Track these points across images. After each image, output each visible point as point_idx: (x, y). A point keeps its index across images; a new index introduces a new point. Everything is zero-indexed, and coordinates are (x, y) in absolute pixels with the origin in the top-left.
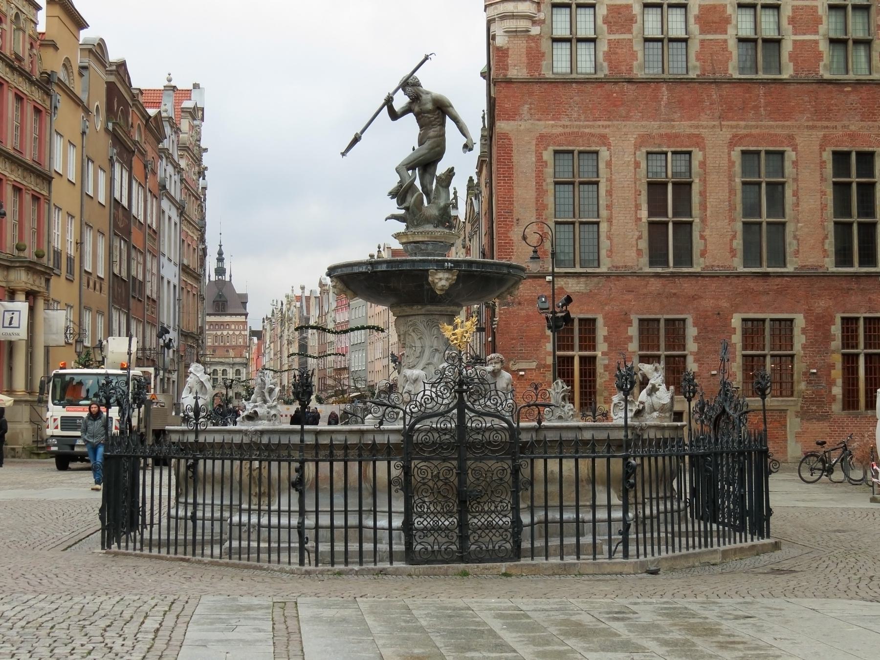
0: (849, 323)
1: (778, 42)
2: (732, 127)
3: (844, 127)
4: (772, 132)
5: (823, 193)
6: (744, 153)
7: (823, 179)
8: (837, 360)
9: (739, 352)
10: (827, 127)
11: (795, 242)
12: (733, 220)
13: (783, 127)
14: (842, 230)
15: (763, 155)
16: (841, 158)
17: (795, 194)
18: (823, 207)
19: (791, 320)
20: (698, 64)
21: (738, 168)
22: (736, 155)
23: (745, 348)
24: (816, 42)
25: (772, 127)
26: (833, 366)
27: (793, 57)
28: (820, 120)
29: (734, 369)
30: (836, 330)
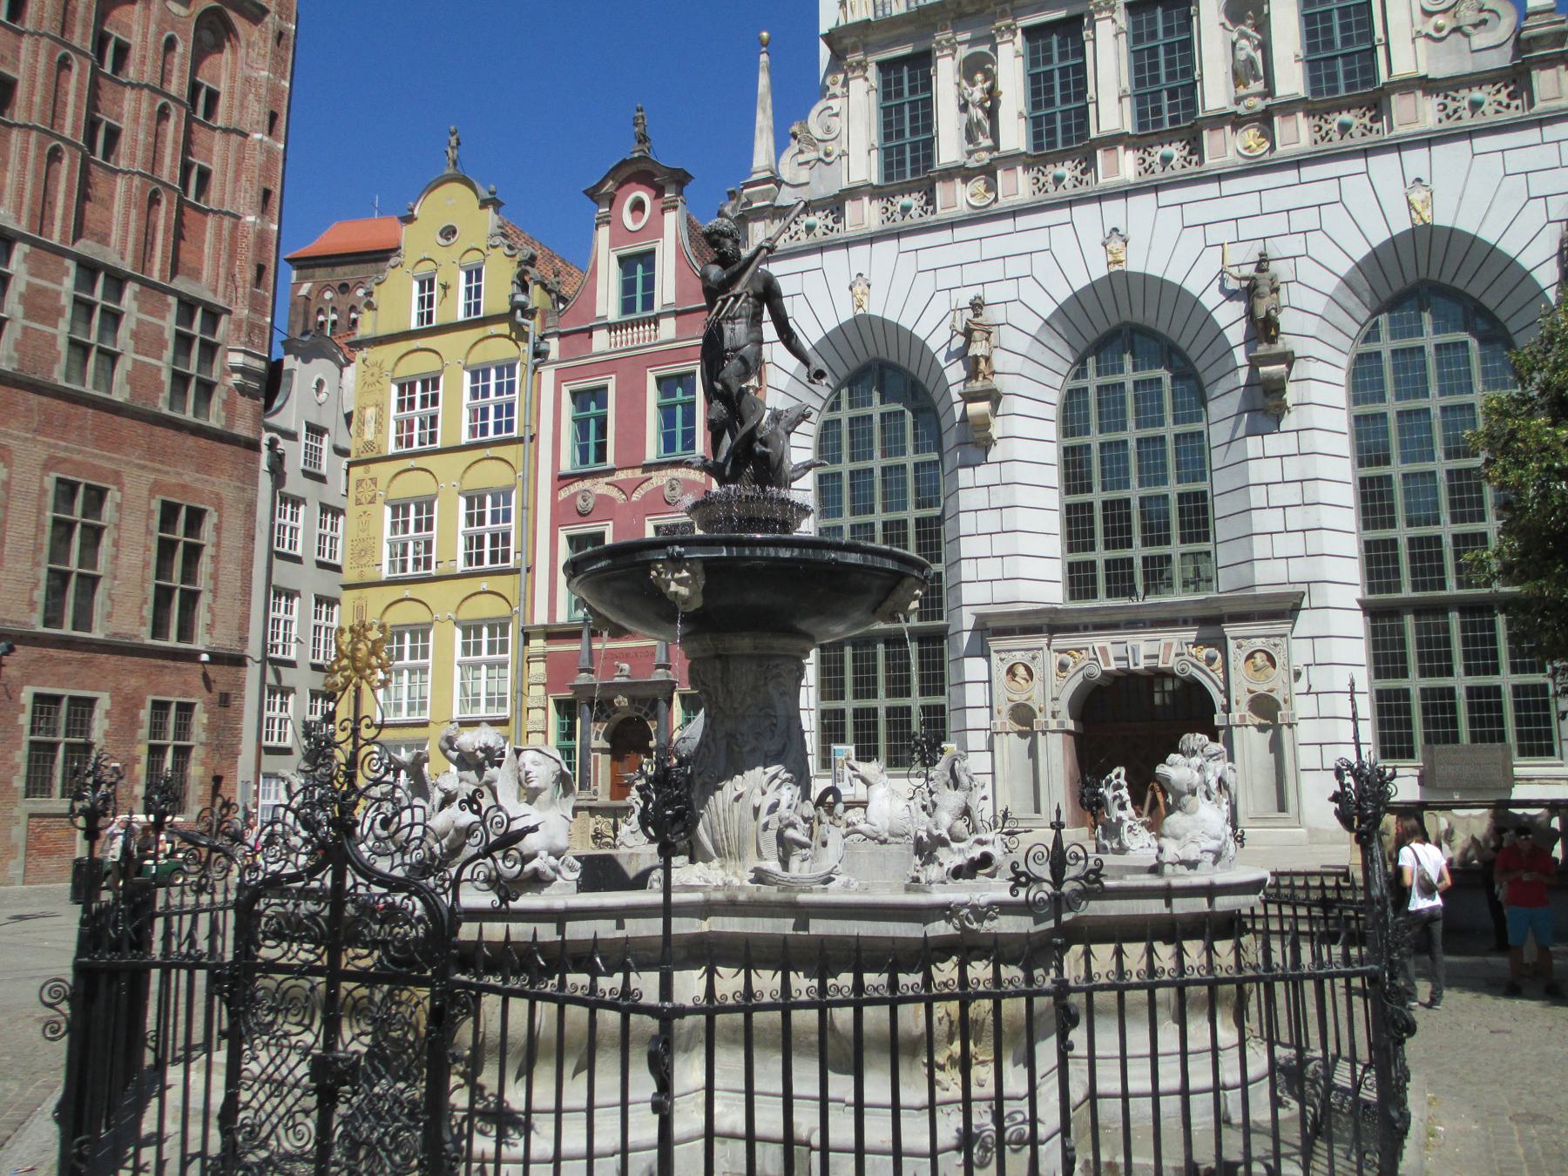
0: (160, 707)
1: (113, 357)
2: (50, 446)
3: (178, 474)
4: (97, 462)
5: (147, 548)
6: (59, 481)
7: (149, 532)
8: (142, 751)
9: (26, 737)
10: (159, 471)
11: (109, 603)
12: (37, 564)
13: (110, 459)
14: (163, 596)
15: (81, 489)
16: (169, 513)
17: (116, 544)
18: (146, 565)
19: (91, 702)
20: (16, 355)
21: (50, 499)
22: (50, 482)
23: (33, 732)
24: (159, 369)
25: (96, 456)
26: (136, 760)
27: (131, 379)
28: (153, 461)
29: (17, 760)
30: (145, 714)
